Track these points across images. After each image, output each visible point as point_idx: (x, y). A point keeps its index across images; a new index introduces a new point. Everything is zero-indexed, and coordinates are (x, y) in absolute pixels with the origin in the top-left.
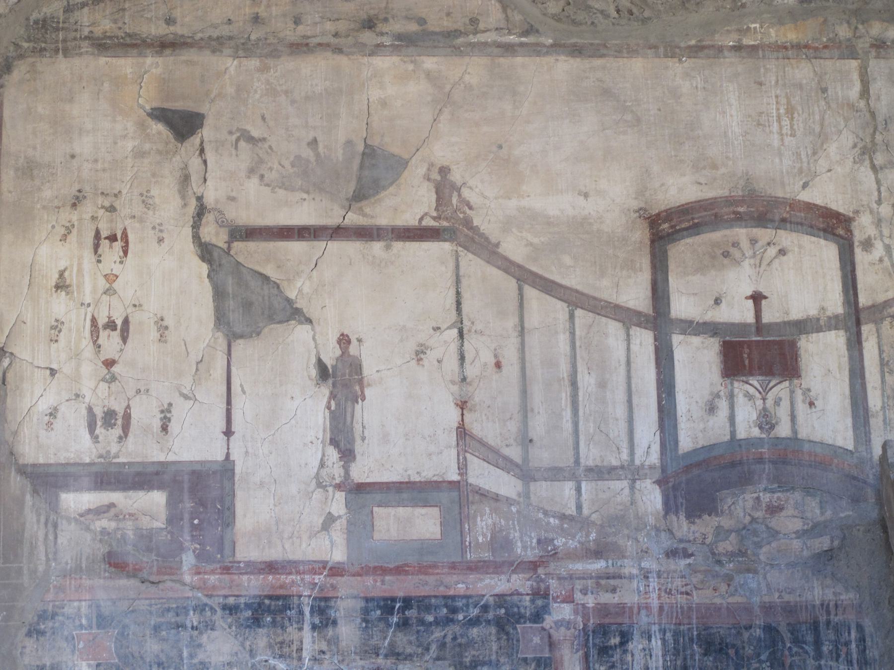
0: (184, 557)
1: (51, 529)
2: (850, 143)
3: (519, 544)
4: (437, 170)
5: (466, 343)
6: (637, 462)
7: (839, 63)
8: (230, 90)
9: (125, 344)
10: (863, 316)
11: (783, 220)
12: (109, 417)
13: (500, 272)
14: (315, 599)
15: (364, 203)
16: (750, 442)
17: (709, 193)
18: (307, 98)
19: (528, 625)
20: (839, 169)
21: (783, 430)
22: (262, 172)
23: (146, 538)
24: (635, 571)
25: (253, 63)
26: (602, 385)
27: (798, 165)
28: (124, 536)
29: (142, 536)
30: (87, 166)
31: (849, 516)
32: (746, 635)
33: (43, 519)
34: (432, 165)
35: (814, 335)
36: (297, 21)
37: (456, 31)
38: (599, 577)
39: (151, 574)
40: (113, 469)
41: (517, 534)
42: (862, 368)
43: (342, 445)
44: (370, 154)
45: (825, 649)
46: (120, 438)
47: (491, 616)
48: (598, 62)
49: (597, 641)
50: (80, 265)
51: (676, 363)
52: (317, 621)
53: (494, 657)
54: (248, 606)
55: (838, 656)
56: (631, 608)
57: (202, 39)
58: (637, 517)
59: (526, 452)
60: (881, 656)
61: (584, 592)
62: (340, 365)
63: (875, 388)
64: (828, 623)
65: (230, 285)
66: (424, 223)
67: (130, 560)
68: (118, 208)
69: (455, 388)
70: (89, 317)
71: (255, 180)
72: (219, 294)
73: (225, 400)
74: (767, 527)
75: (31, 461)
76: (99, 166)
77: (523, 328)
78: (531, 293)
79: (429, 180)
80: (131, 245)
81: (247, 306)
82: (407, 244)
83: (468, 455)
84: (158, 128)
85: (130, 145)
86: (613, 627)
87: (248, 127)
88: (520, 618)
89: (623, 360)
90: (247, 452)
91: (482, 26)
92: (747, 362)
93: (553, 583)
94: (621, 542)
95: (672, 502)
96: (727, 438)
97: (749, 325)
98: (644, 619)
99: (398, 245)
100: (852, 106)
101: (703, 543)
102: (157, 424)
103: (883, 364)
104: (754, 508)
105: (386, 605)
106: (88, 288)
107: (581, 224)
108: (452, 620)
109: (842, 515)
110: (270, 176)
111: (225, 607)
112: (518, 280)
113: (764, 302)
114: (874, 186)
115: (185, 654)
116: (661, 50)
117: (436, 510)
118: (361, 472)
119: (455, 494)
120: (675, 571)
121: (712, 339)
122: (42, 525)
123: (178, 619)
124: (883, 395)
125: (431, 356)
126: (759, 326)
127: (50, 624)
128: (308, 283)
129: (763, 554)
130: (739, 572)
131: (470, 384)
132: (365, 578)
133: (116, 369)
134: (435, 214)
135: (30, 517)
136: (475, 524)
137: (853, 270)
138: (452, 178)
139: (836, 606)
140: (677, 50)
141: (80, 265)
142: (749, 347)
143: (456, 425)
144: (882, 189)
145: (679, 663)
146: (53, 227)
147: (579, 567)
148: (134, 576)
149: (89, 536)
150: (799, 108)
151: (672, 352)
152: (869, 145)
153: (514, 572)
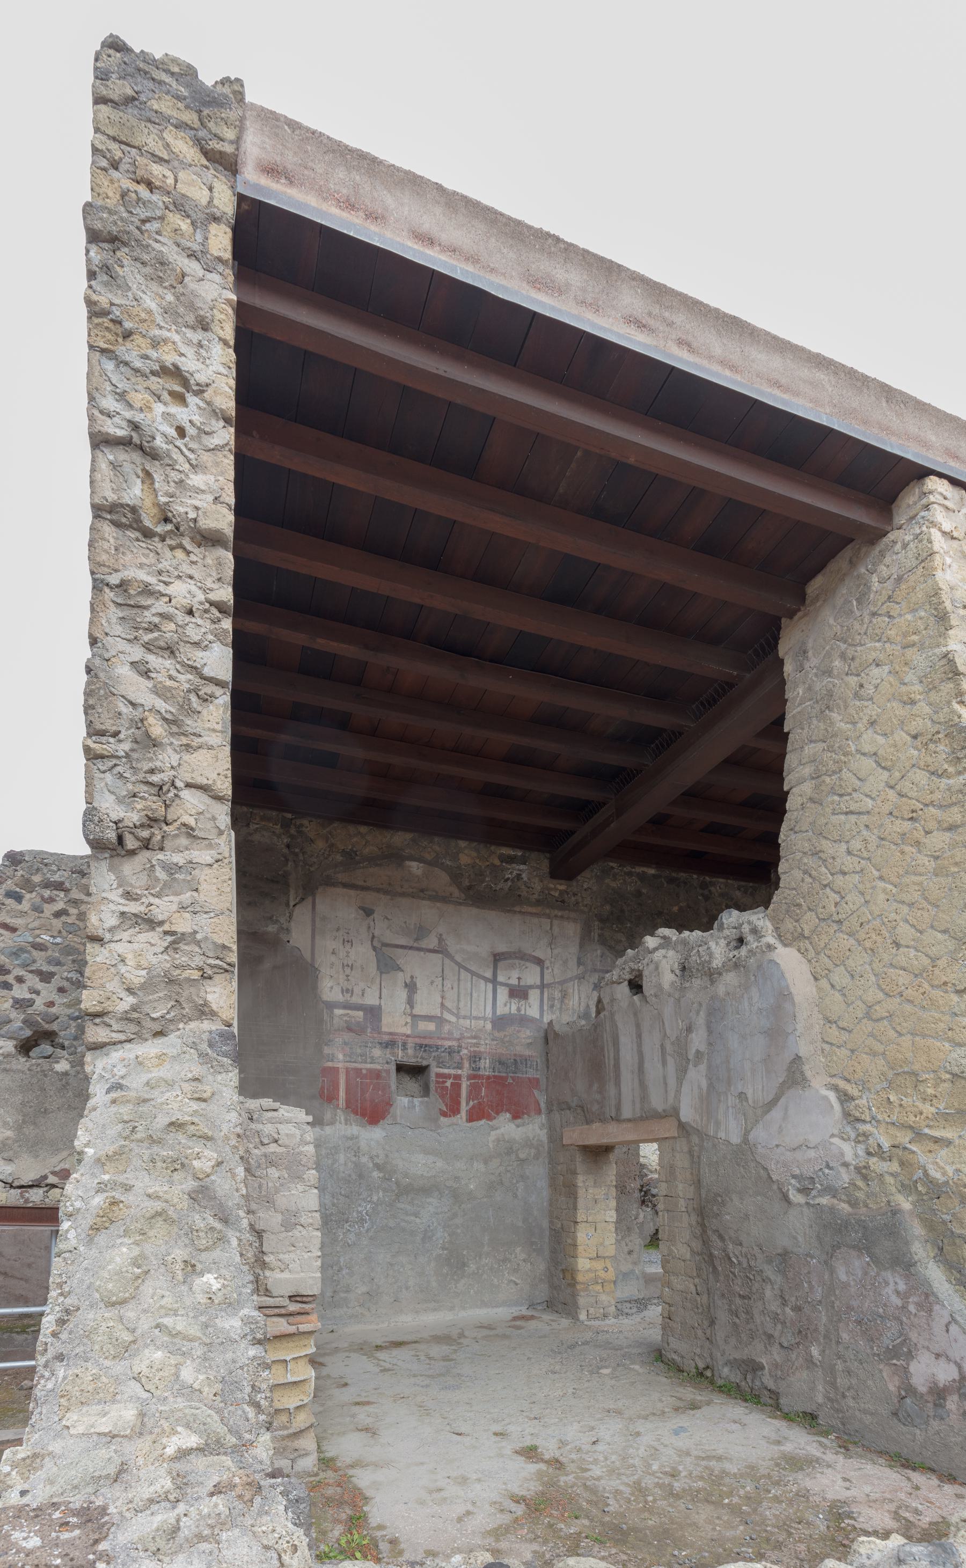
78: (462, 970)
118: (417, 1011)
125: (435, 984)
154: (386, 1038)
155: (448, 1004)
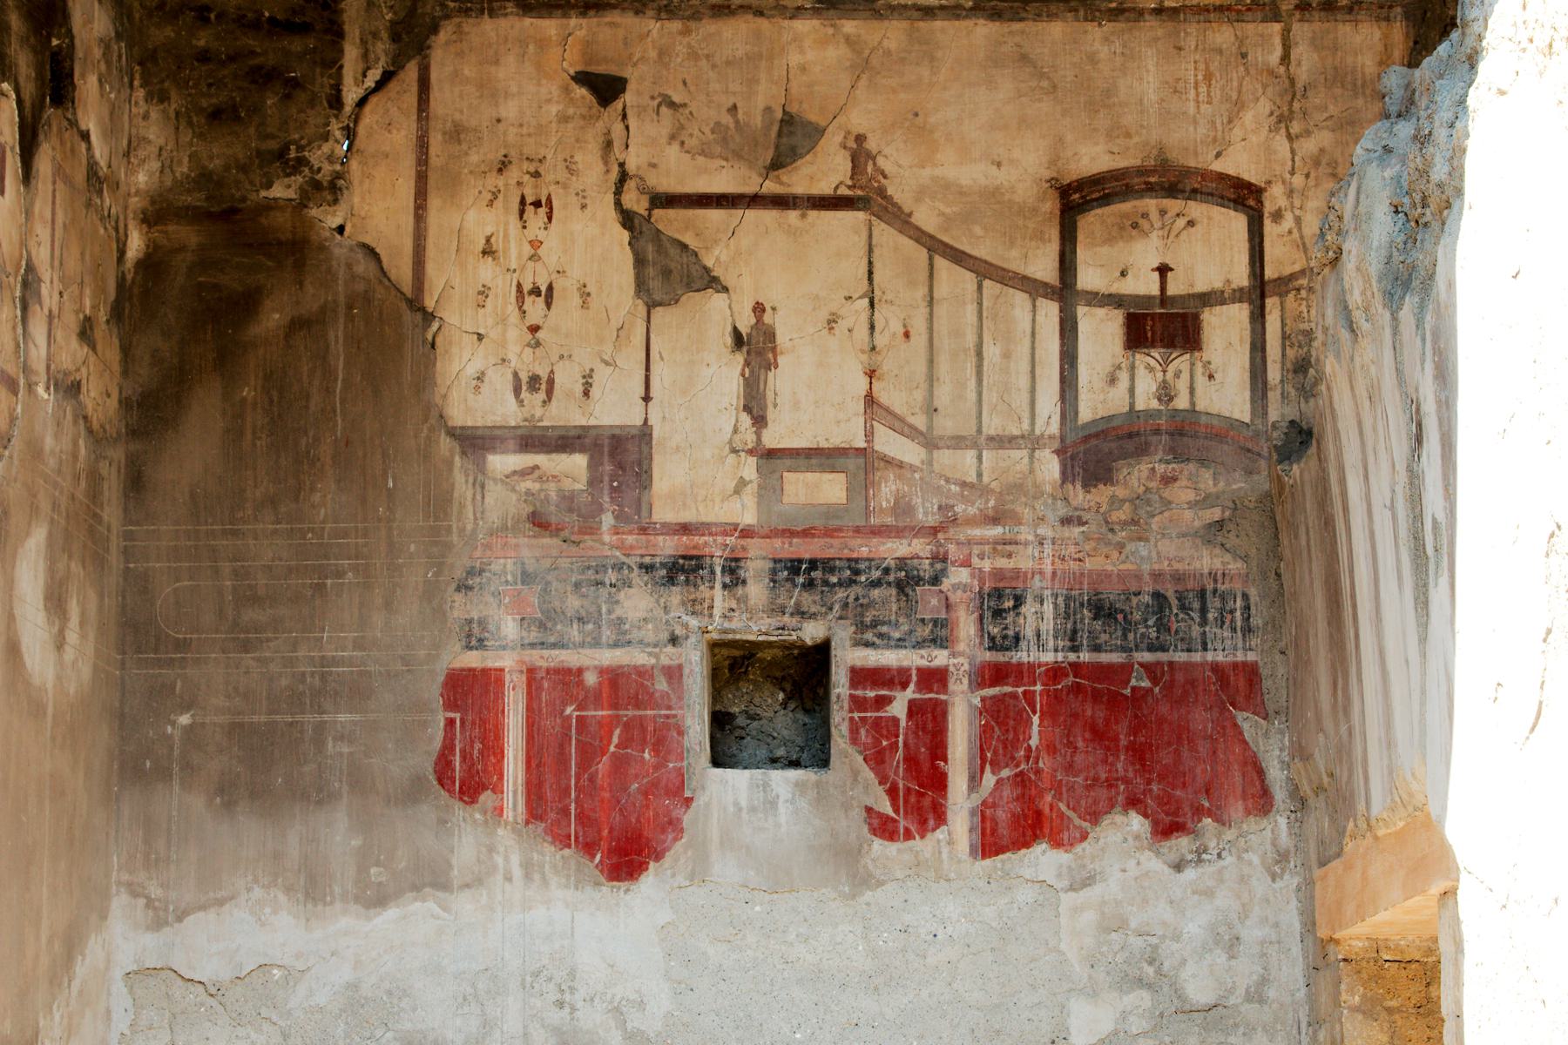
1: (479, 490)
2: (1267, 111)
3: (921, 510)
4: (853, 138)
6: (1038, 432)
7: (1261, 27)
8: (653, 54)
9: (549, 308)
10: (1268, 288)
11: (1194, 191)
12: (534, 380)
13: (911, 242)
14: (726, 559)
15: (781, 171)
16: (1149, 414)
18: (728, 63)
19: (927, 587)
20: (1254, 139)
21: (1182, 403)
22: (683, 138)
23: (568, 499)
24: (1030, 538)
25: (676, 25)
26: (1007, 355)
28: (547, 497)
29: (564, 497)
31: (1241, 488)
32: (1135, 600)
33: (471, 479)
34: (849, 133)
35: (1218, 308)
38: (996, 543)
40: (537, 432)
41: (919, 500)
42: (1264, 341)
43: (755, 411)
44: (789, 122)
45: (1210, 616)
46: (544, 402)
47: (891, 578)
48: (1017, 26)
49: (992, 604)
50: (506, 231)
51: (1080, 334)
52: (727, 580)
53: (893, 618)
54: (663, 565)
55: (1223, 623)
58: (1035, 485)
59: (931, 420)
61: (981, 557)
62: (754, 333)
63: (1275, 362)
64: (1215, 591)
66: (839, 192)
67: (553, 520)
68: (543, 173)
69: (864, 357)
70: (515, 283)
71: (676, 147)
72: (640, 262)
73: (644, 366)
74: (1161, 497)
75: (459, 423)
76: (525, 131)
77: (932, 298)
78: (941, 263)
79: (845, 148)
81: (666, 273)
82: (823, 213)
84: (581, 92)
85: (554, 109)
86: (1008, 591)
87: (670, 93)
88: (918, 580)
90: (664, 417)
92: (1149, 334)
93: (952, 548)
94: (1019, 509)
95: (1069, 471)
96: (1127, 409)
97: (1154, 297)
98: (1037, 583)
99: (813, 214)
100: (1271, 73)
101: (1097, 511)
102: (579, 389)
103: (1285, 337)
104: (1149, 478)
105: (792, 566)
107: (992, 194)
108: (855, 582)
109: (1234, 487)
110: (692, 143)
111: (641, 566)
113: (1169, 274)
114: (1289, 155)
115: (604, 610)
116: (1082, 13)
118: (771, 439)
119: (861, 461)
120: (1069, 538)
121: (1116, 311)
122: (470, 486)
123: (598, 577)
124: (1283, 369)
125: (842, 326)
126: (1164, 299)
127: (478, 580)
128: (725, 251)
129: (1155, 523)
130: (1131, 539)
131: (879, 353)
132: (775, 540)
133: (540, 335)
134: (850, 183)
135: (459, 477)
137: (1262, 242)
139: (1224, 574)
140: (1097, 14)
141: (506, 231)
142: (1153, 320)
143: (864, 393)
144: (1297, 159)
145: (1069, 626)
146: (480, 192)
147: (977, 532)
148: (557, 536)
149: (514, 497)
151: (1076, 323)
153: (915, 536)
154: (667, 547)
155: (887, 394)
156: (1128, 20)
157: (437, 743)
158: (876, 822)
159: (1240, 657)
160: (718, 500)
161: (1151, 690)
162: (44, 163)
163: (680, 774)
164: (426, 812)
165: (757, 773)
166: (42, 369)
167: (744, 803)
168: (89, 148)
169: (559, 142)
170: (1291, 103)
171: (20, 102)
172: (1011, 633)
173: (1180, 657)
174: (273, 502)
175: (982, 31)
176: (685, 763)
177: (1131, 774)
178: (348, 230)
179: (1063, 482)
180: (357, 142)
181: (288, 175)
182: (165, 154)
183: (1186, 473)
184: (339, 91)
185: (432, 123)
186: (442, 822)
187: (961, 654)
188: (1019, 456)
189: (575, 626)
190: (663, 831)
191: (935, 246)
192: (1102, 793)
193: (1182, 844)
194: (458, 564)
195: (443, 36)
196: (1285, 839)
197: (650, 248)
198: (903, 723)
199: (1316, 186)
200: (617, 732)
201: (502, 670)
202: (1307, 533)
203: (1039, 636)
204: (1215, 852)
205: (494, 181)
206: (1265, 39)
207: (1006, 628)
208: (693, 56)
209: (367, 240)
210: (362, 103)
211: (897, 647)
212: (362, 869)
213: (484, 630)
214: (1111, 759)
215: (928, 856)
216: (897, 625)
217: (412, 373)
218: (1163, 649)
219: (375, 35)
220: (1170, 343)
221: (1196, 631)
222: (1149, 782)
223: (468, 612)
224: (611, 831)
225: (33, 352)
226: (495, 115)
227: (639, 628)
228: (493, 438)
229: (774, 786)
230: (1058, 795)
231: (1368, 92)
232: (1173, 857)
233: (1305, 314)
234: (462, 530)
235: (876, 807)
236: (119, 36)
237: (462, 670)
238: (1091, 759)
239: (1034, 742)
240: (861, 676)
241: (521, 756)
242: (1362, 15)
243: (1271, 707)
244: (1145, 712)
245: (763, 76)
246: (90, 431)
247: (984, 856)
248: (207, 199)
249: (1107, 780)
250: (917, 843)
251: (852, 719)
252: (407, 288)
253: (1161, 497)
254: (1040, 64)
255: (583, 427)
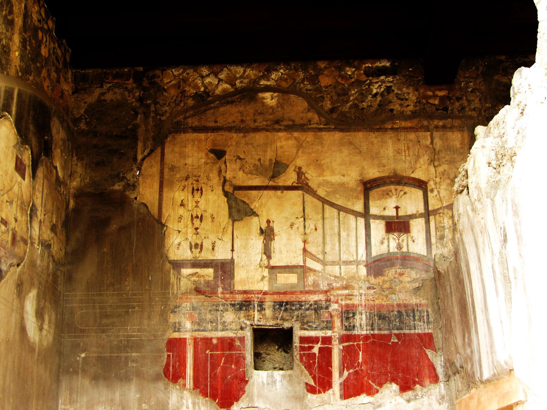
0: (219, 289)
1: (178, 280)
2: (427, 158)
5: (306, 222)
6: (359, 260)
7: (424, 133)
8: (234, 143)
11: (406, 183)
12: (196, 245)
17: (383, 175)
18: (258, 146)
19: (324, 310)
21: (404, 249)
23: (207, 283)
24: (357, 294)
25: (242, 135)
26: (348, 235)
27: (410, 166)
28: (200, 282)
29: (206, 283)
30: (190, 167)
32: (392, 314)
33: (176, 277)
34: (296, 167)
36: (255, 121)
37: (304, 124)
38: (347, 296)
39: (209, 294)
40: (197, 262)
41: (321, 282)
46: (200, 252)
47: (312, 307)
48: (348, 134)
49: (345, 315)
50: (188, 198)
52: (259, 309)
53: (313, 320)
54: (238, 304)
55: (420, 320)
56: (356, 305)
57: (226, 127)
58: (359, 277)
60: (434, 320)
61: (342, 300)
64: (417, 310)
65: (233, 204)
66: (293, 185)
67: (202, 289)
69: (302, 236)
70: (190, 215)
71: (241, 172)
72: (230, 207)
74: (399, 280)
75: (172, 259)
77: (324, 218)
78: (327, 207)
79: (295, 171)
80: (203, 192)
81: (239, 211)
83: (306, 258)
84: (211, 155)
85: (203, 161)
87: (240, 155)
88: (322, 308)
89: (355, 228)
90: (238, 257)
91: (312, 122)
93: (332, 297)
94: (353, 284)
95: (369, 272)
97: (394, 216)
98: (360, 308)
99: (285, 192)
100: (427, 147)
102: (211, 247)
103: (436, 228)
104: (395, 274)
105: (280, 304)
106: (190, 205)
107: (342, 185)
108: (301, 309)
110: (246, 170)
111: (231, 304)
112: (322, 202)
113: (399, 209)
114: (434, 172)
115: (219, 319)
116: (368, 129)
117: (296, 274)
118: (273, 263)
119: (302, 270)
120: (370, 294)
122: (176, 279)
123: (217, 308)
125: (295, 227)
126: (397, 217)
127: (178, 309)
128: (257, 203)
130: (390, 294)
131: (307, 235)
132: (274, 296)
133: (198, 231)
134: (297, 182)
135: (172, 275)
136: (308, 279)
138: (302, 171)
139: (420, 305)
142: (394, 223)
148: (203, 295)
150: (411, 148)
152: (433, 159)
153: (320, 294)
154: (239, 298)
155: (311, 249)
156: (383, 131)
157: (165, 363)
158: (309, 388)
159: (426, 331)
160: (256, 283)
161: (398, 342)
162: (40, 173)
163: (244, 372)
164: (161, 385)
165: (270, 372)
166: (37, 238)
167: (265, 382)
168: (57, 172)
169: (205, 171)
170: (434, 156)
171: (32, 152)
172: (352, 325)
173: (407, 332)
174: (112, 284)
175: (338, 135)
176: (246, 369)
177: (392, 371)
178: (138, 198)
179: (368, 276)
180: (141, 172)
181: (120, 182)
182: (82, 176)
183: (407, 272)
184: (136, 156)
185: (165, 166)
186: (166, 389)
187: (335, 332)
188: (353, 267)
189: (210, 324)
190: (239, 392)
191: (324, 201)
192: (383, 377)
193: (410, 393)
194: (172, 304)
195: (169, 139)
196: (443, 391)
197: (233, 203)
198: (317, 355)
199: (444, 181)
200: (223, 359)
201: (186, 339)
202: (450, 287)
203: (361, 326)
204: (420, 396)
205: (184, 183)
206: (425, 137)
207: (350, 323)
208: (247, 144)
209: (144, 202)
210: (143, 159)
211: (315, 330)
212: (140, 405)
213: (180, 325)
214: (385, 366)
215: (326, 399)
216: (315, 322)
217: (158, 243)
218: (402, 329)
219: (148, 139)
220: (400, 231)
221: (412, 323)
222: (398, 373)
223: (175, 320)
224: (221, 391)
225: (34, 233)
226: (184, 162)
227: (230, 325)
228: (183, 264)
229: (275, 376)
230: (369, 378)
231: (458, 153)
232: (407, 397)
233: (442, 221)
234: (173, 293)
235: (309, 383)
236: (68, 140)
237: (173, 339)
238: (379, 366)
239: (360, 360)
240: (303, 340)
241: (192, 367)
242: (455, 130)
243: (437, 347)
244: (396, 350)
245: (269, 150)
246: (54, 261)
247: (345, 399)
248: (94, 189)
249: (384, 372)
250: (322, 395)
251: (300, 354)
252: (156, 216)
253: (399, 280)
254: (356, 145)
255: (212, 260)
